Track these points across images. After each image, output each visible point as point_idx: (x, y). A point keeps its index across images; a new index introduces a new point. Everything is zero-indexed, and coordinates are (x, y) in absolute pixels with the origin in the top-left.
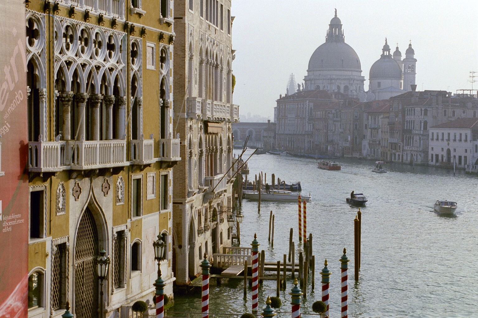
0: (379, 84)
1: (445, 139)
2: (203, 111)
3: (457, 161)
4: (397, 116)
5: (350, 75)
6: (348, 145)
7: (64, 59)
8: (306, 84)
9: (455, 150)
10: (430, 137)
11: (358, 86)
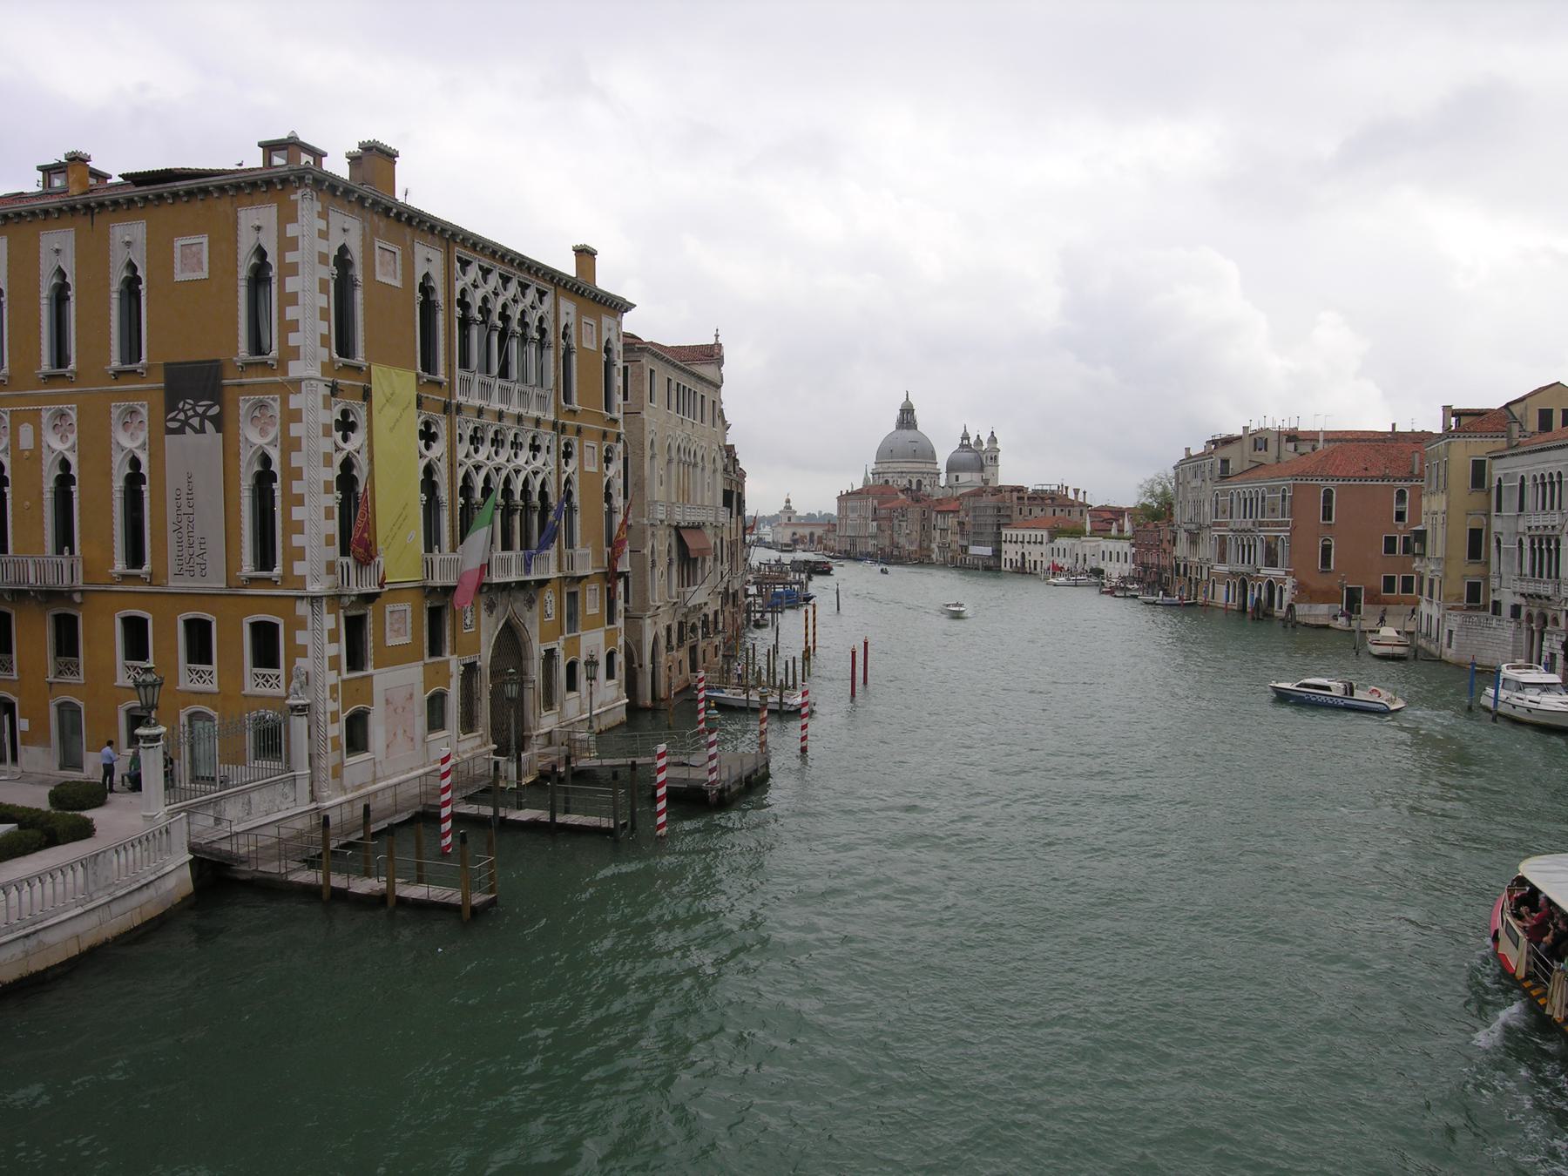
0: (957, 477)
2: (669, 513)
3: (1032, 566)
6: (914, 548)
7: (470, 462)
10: (1003, 539)
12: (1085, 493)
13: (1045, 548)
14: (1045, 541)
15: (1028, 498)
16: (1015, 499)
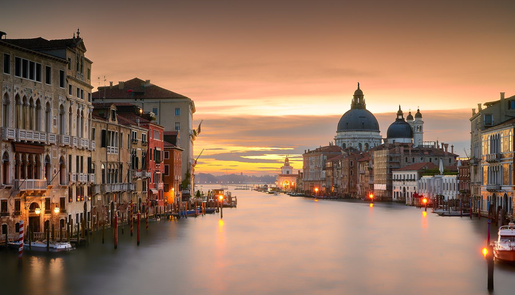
0: (394, 141)
1: (405, 179)
4: (373, 163)
5: (369, 135)
6: (345, 187)
8: (335, 142)
9: (408, 187)
10: (393, 178)
11: (377, 143)
12: (452, 147)
13: (415, 184)
14: (416, 179)
15: (412, 151)
16: (402, 151)
